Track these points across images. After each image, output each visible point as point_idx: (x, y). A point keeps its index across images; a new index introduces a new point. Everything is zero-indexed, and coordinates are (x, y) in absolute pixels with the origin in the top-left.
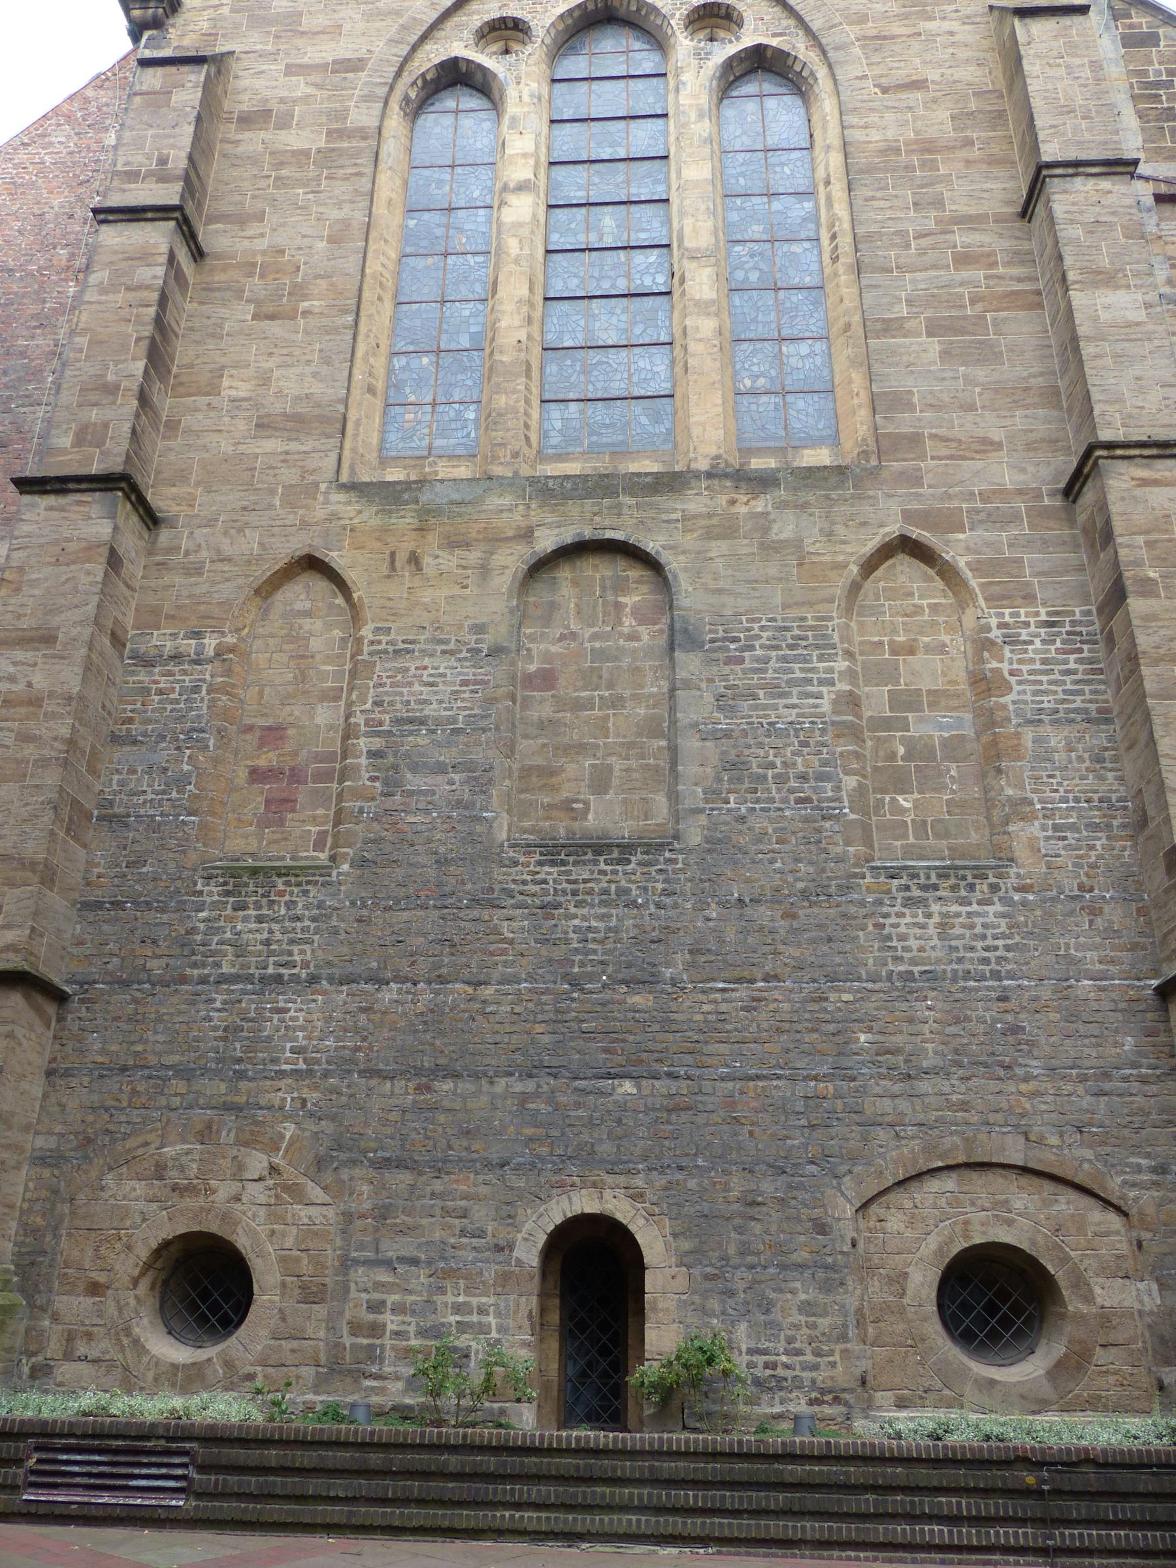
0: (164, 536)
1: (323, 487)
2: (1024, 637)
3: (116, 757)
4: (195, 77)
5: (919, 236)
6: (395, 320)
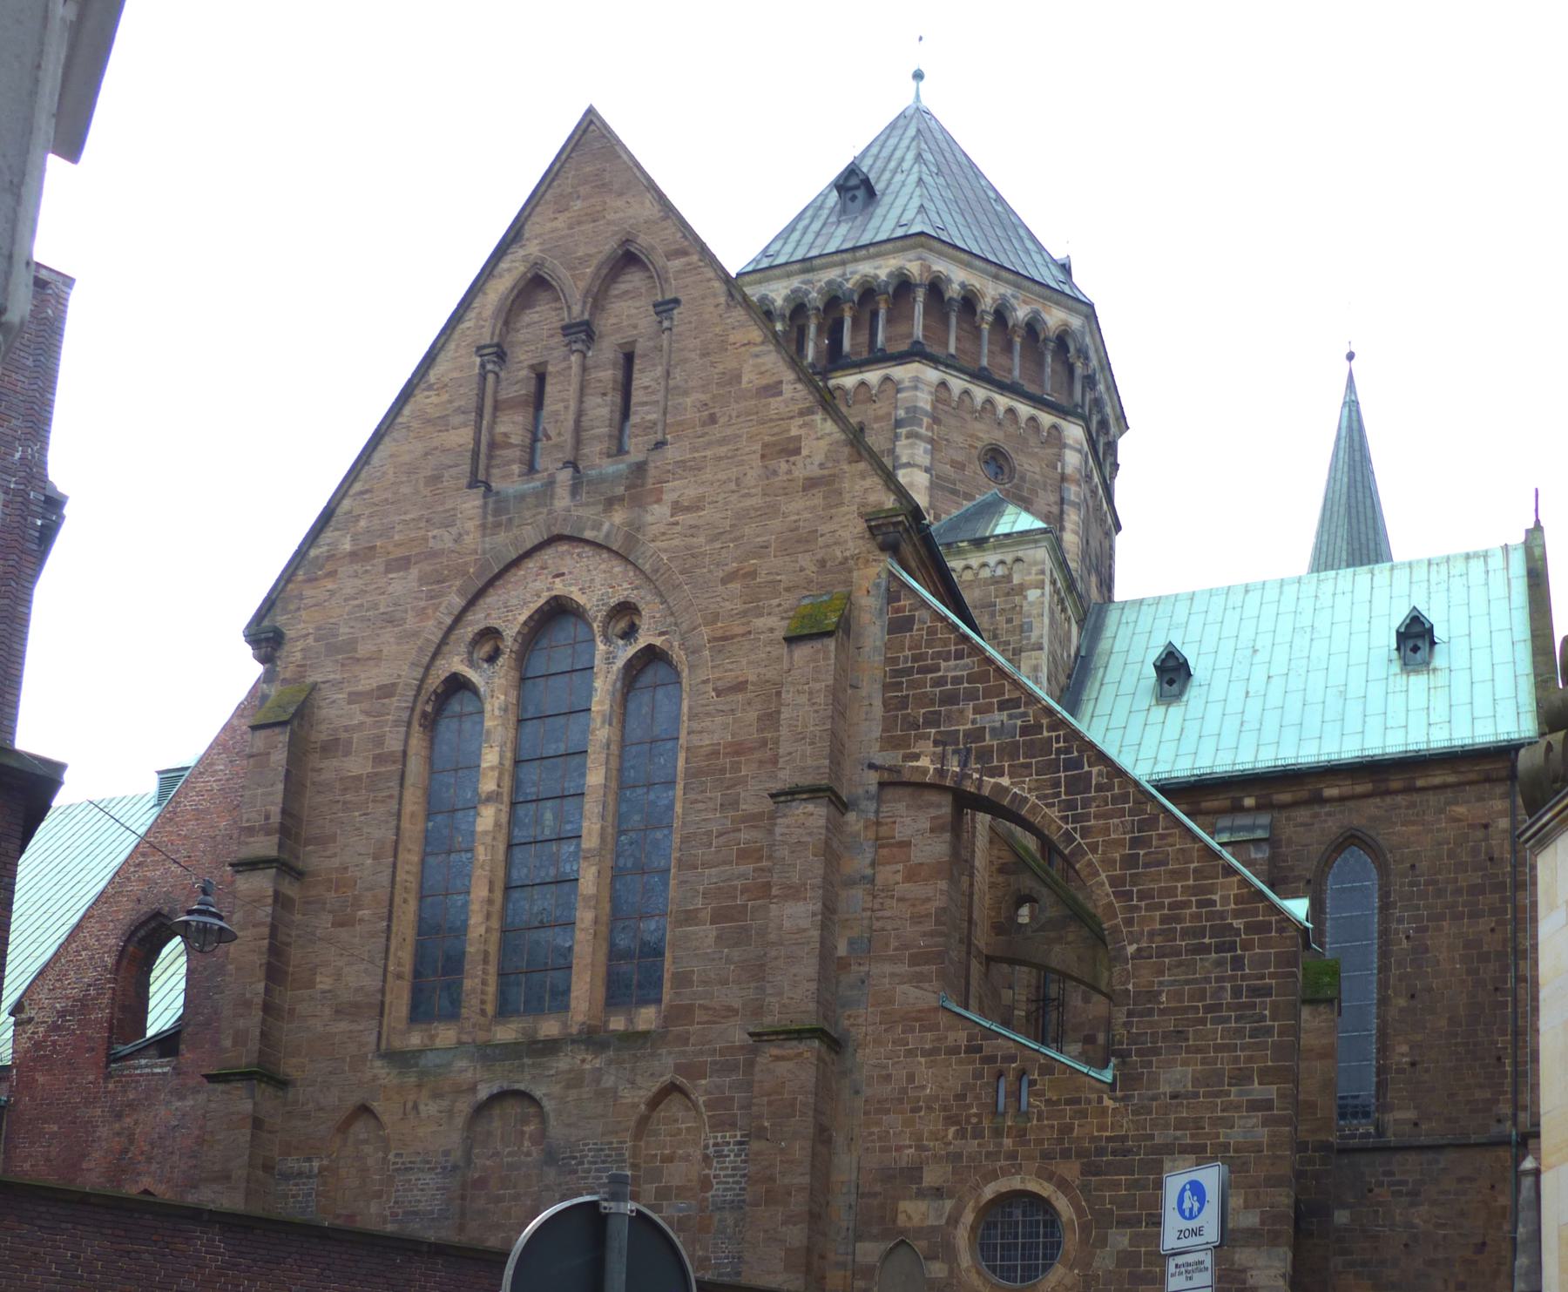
2: (726, 1153)
5: (720, 835)
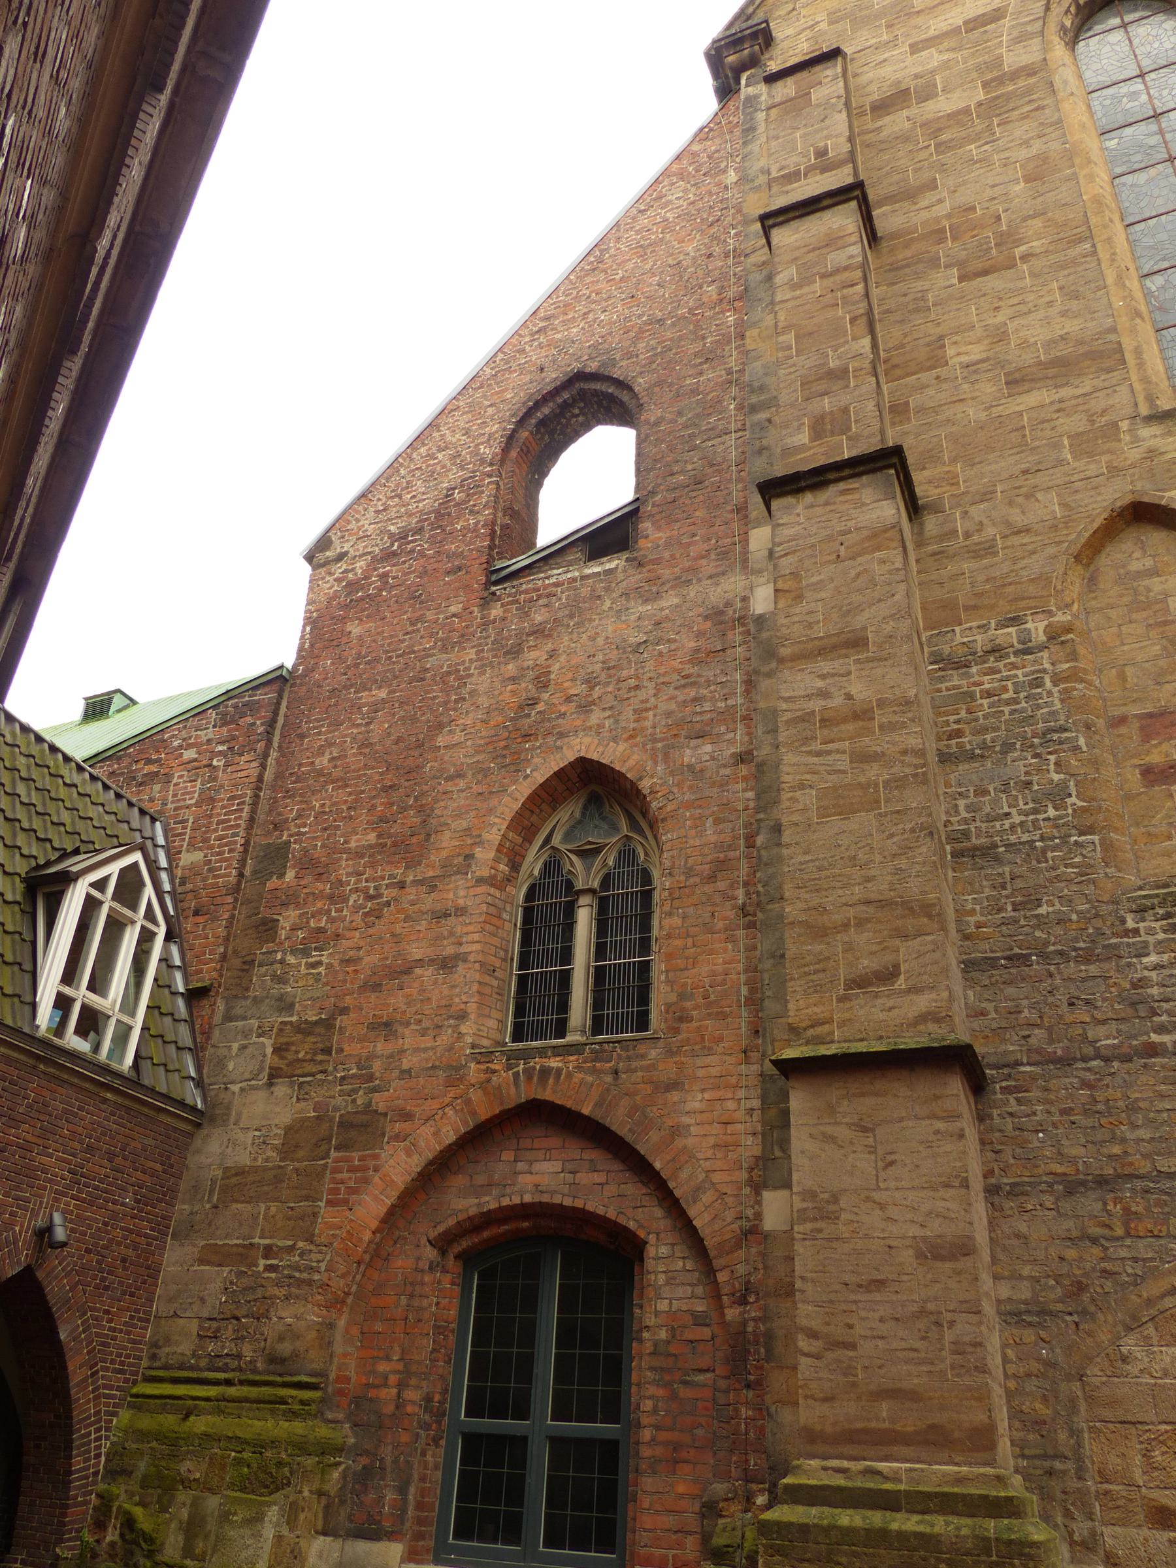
0: (931, 524)
1: (1124, 425)
3: (953, 778)
4: (829, 72)
6: (1132, 244)
